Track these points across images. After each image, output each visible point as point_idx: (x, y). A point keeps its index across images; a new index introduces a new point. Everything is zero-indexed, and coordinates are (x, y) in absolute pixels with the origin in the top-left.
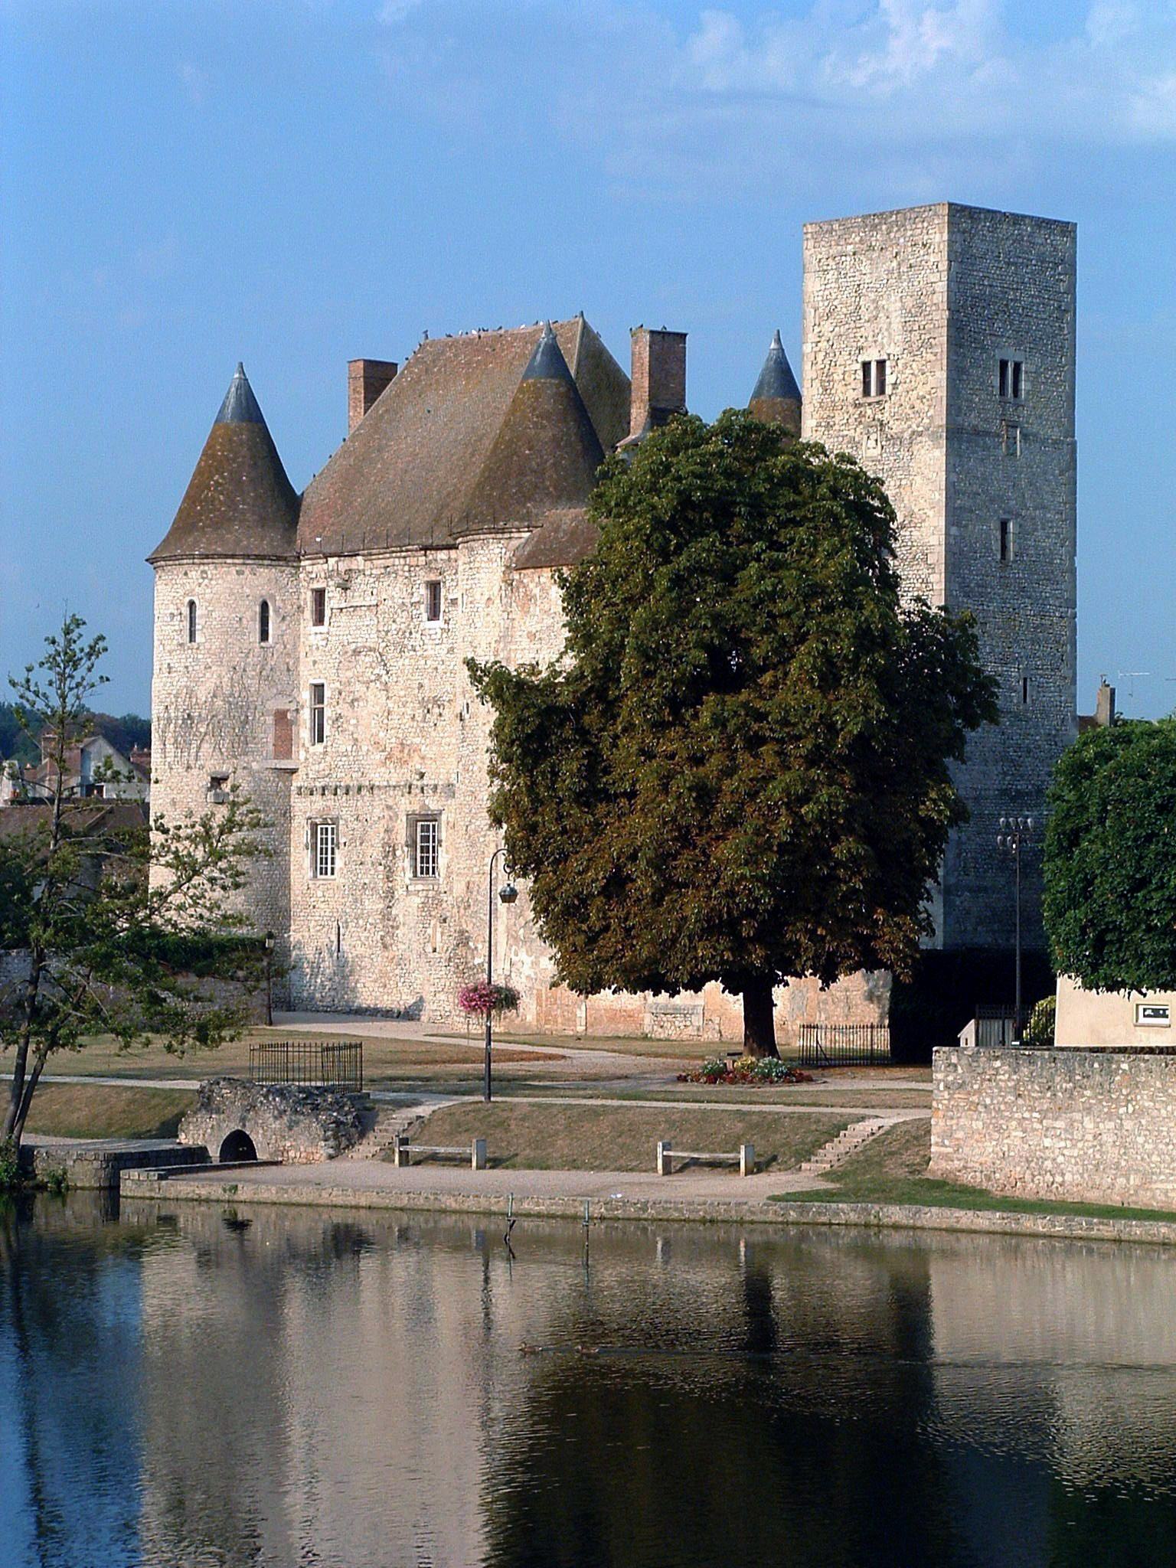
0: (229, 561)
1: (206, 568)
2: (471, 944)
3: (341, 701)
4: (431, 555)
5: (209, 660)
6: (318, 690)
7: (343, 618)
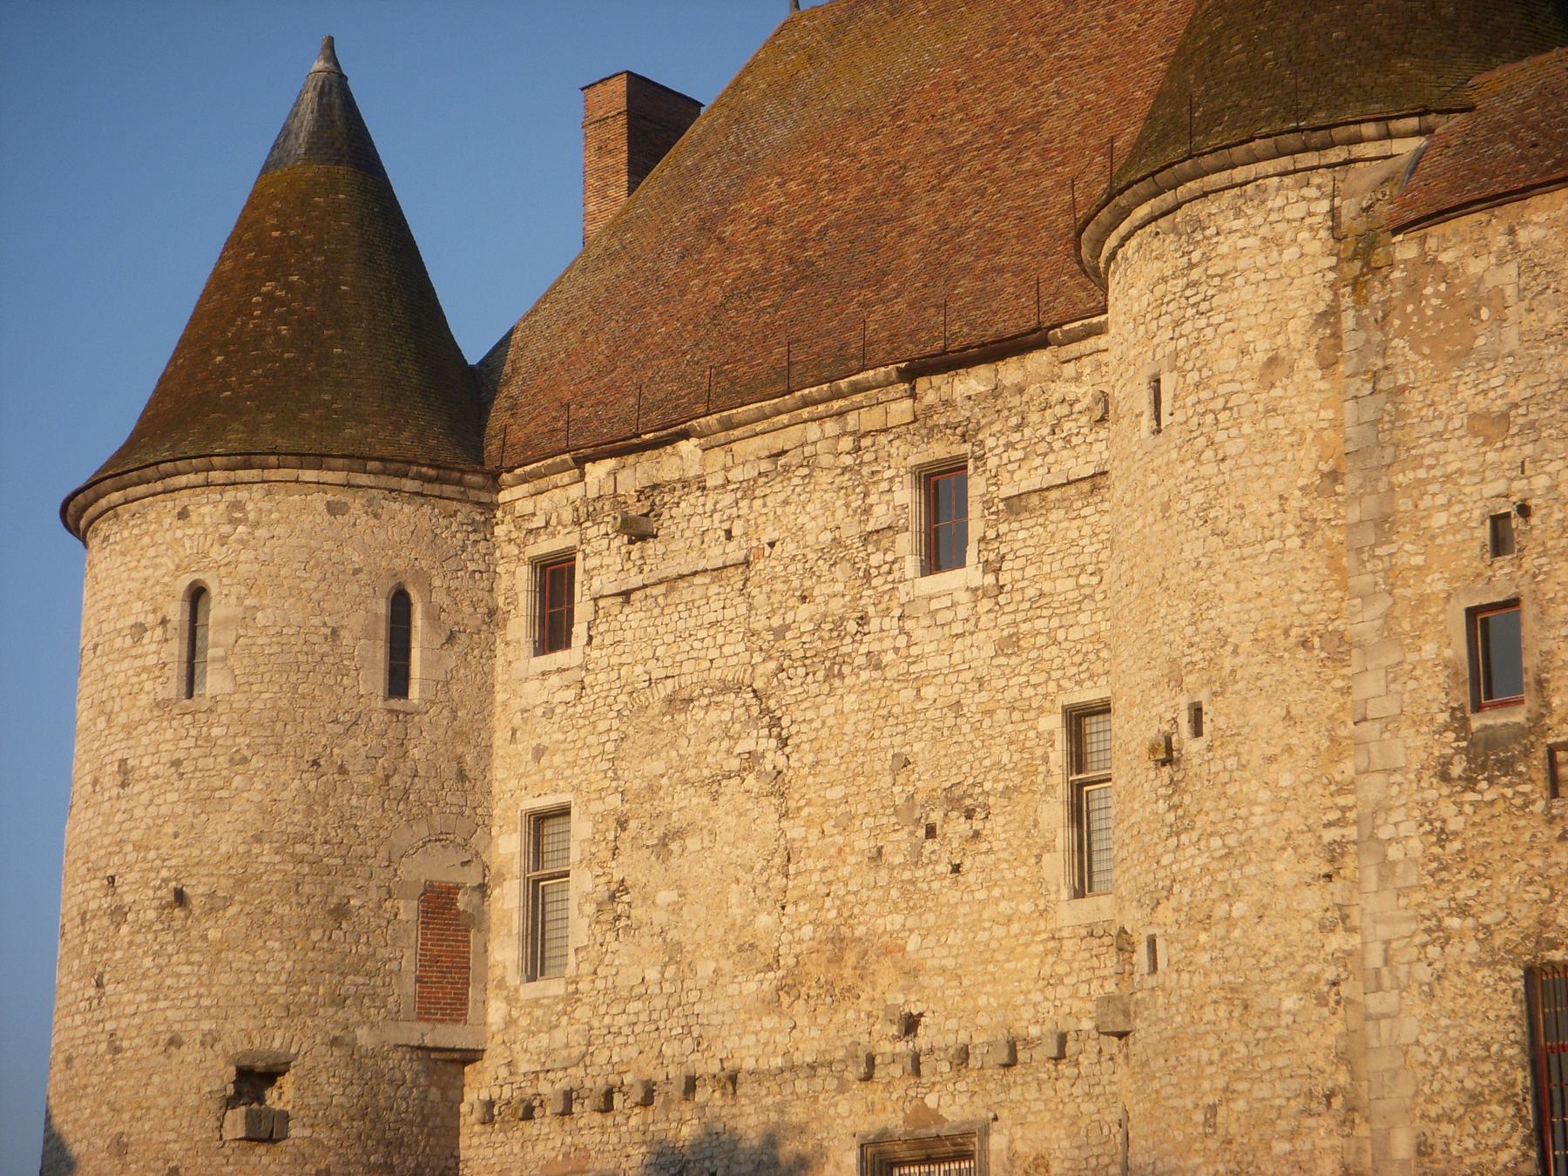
1: (242, 495)
3: (625, 847)
4: (932, 389)
5: (243, 741)
6: (541, 822)
7: (634, 617)
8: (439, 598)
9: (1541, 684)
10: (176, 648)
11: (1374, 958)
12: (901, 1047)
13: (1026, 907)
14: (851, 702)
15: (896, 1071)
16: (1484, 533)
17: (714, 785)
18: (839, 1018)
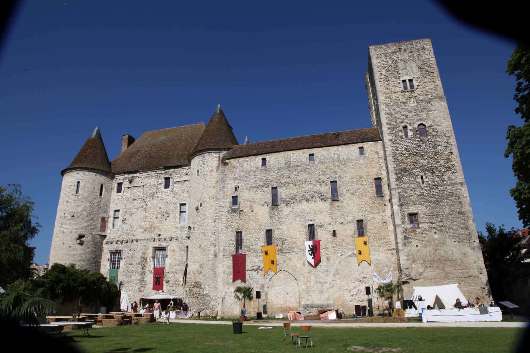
0: (93, 171)
1: (85, 172)
2: (202, 286)
3: (126, 215)
5: (83, 199)
7: (129, 190)
8: (106, 186)
9: (239, 204)
10: (75, 188)
11: (220, 230)
12: (158, 238)
13: (174, 224)
14: (155, 201)
15: (157, 240)
16: (234, 189)
17: (138, 209)
18: (151, 234)
